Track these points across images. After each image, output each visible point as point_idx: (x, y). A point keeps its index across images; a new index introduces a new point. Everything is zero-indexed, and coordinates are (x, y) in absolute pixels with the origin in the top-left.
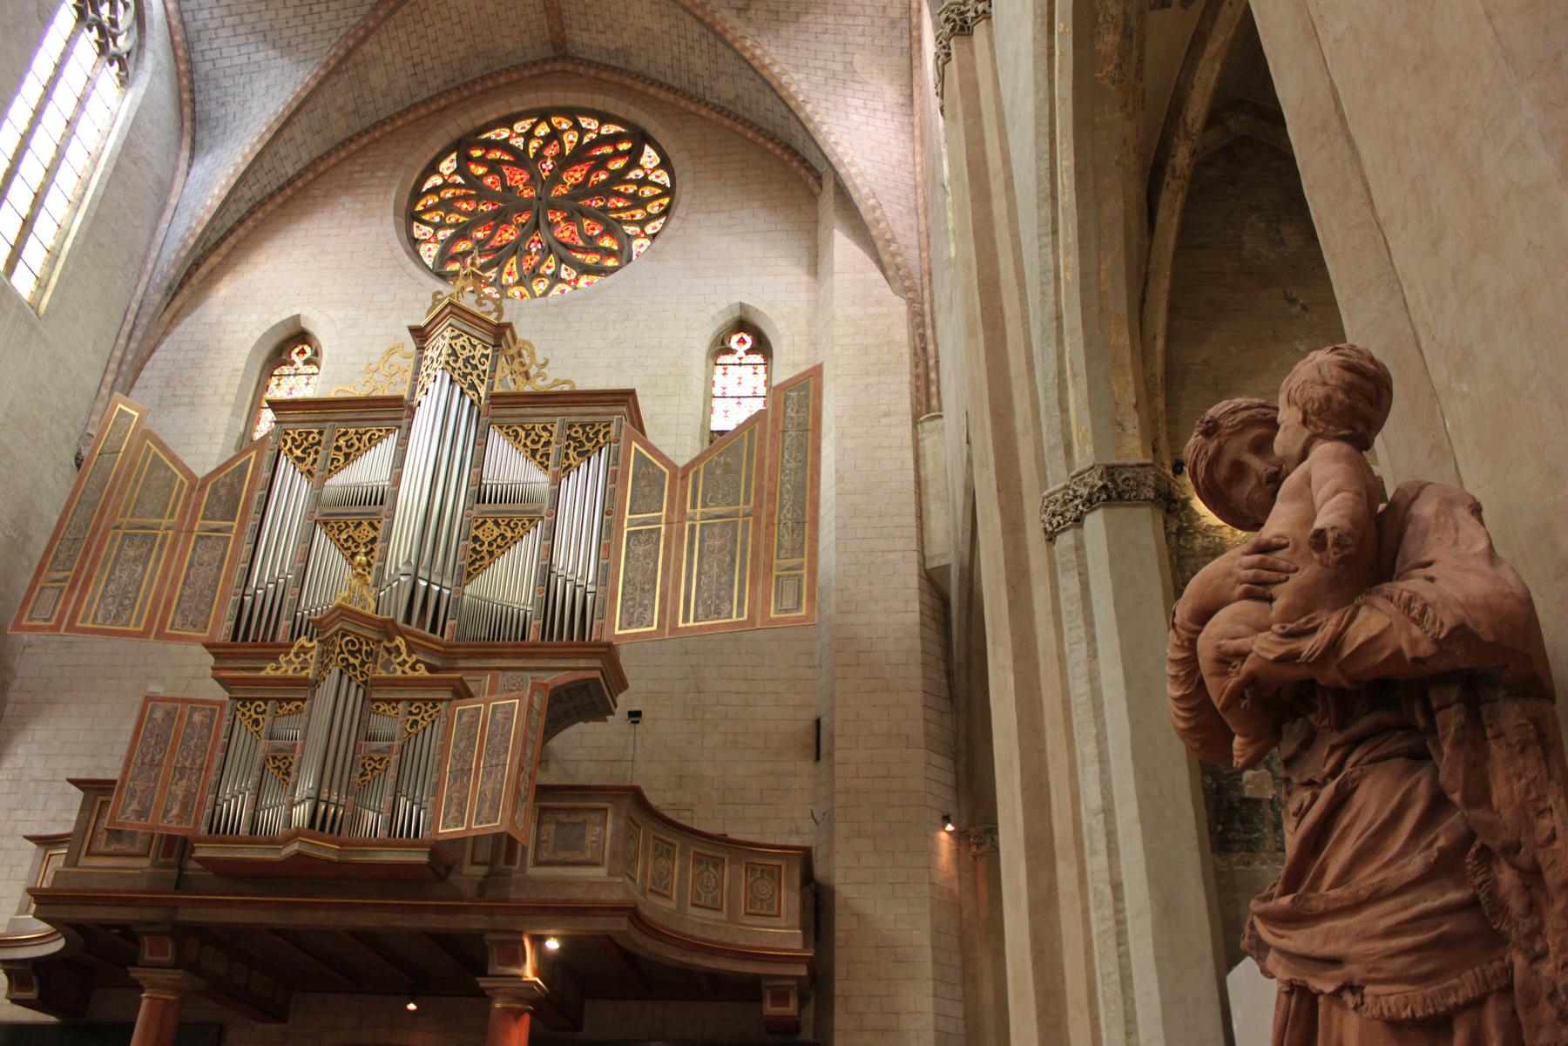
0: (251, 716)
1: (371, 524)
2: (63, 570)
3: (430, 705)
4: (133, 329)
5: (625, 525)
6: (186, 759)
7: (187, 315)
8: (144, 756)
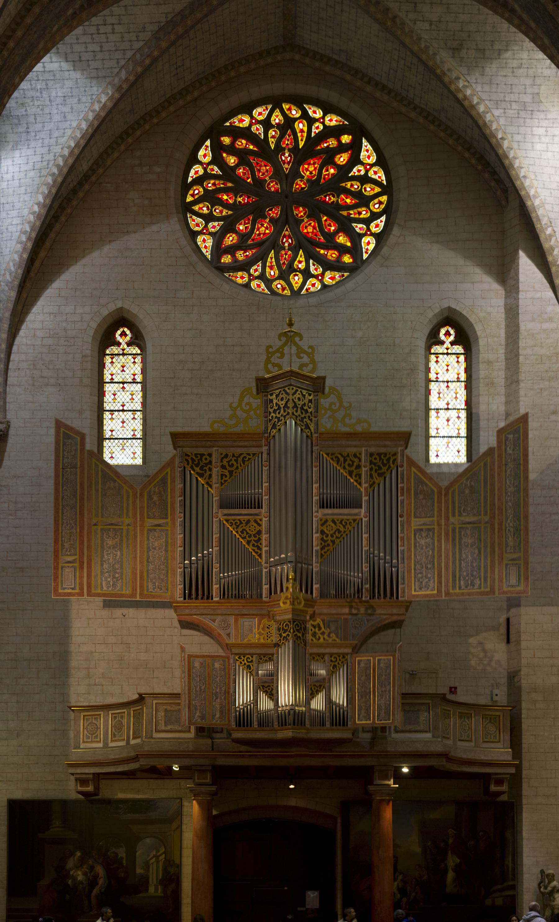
0: (245, 664)
1: (255, 521)
2: (70, 555)
3: (341, 656)
5: (412, 525)
6: (217, 688)
8: (196, 687)
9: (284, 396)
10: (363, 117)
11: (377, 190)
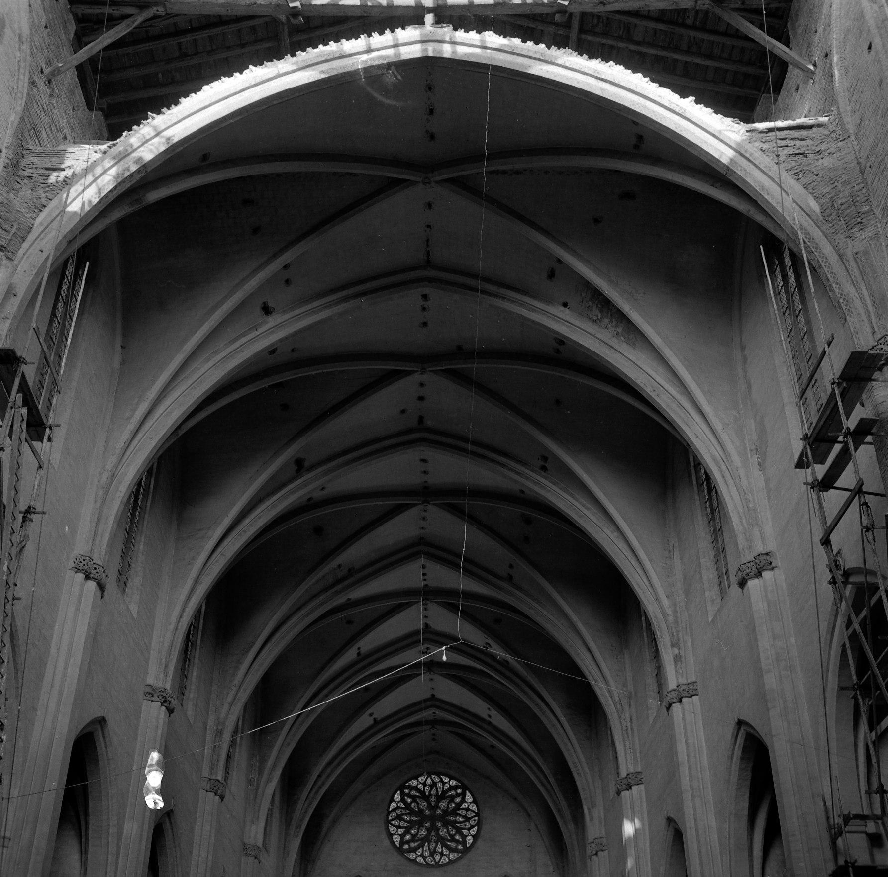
10: (466, 782)
11: (473, 814)
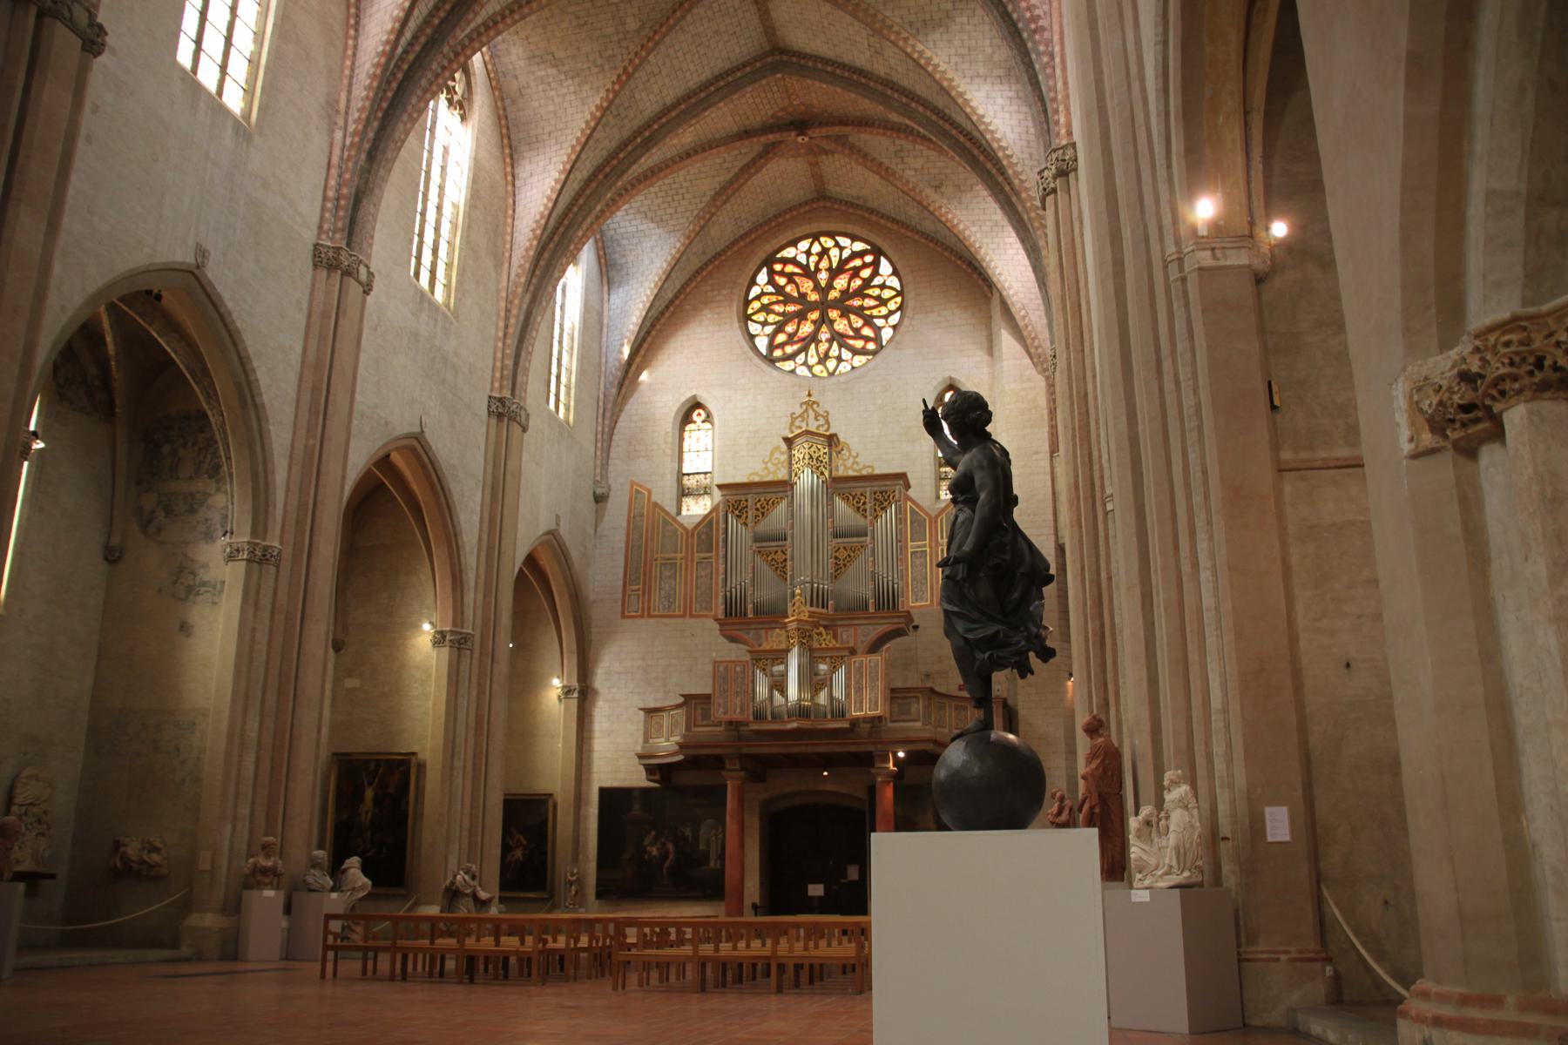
4: (604, 410)
7: (630, 397)
9: (802, 450)
10: (879, 242)
11: (894, 293)
